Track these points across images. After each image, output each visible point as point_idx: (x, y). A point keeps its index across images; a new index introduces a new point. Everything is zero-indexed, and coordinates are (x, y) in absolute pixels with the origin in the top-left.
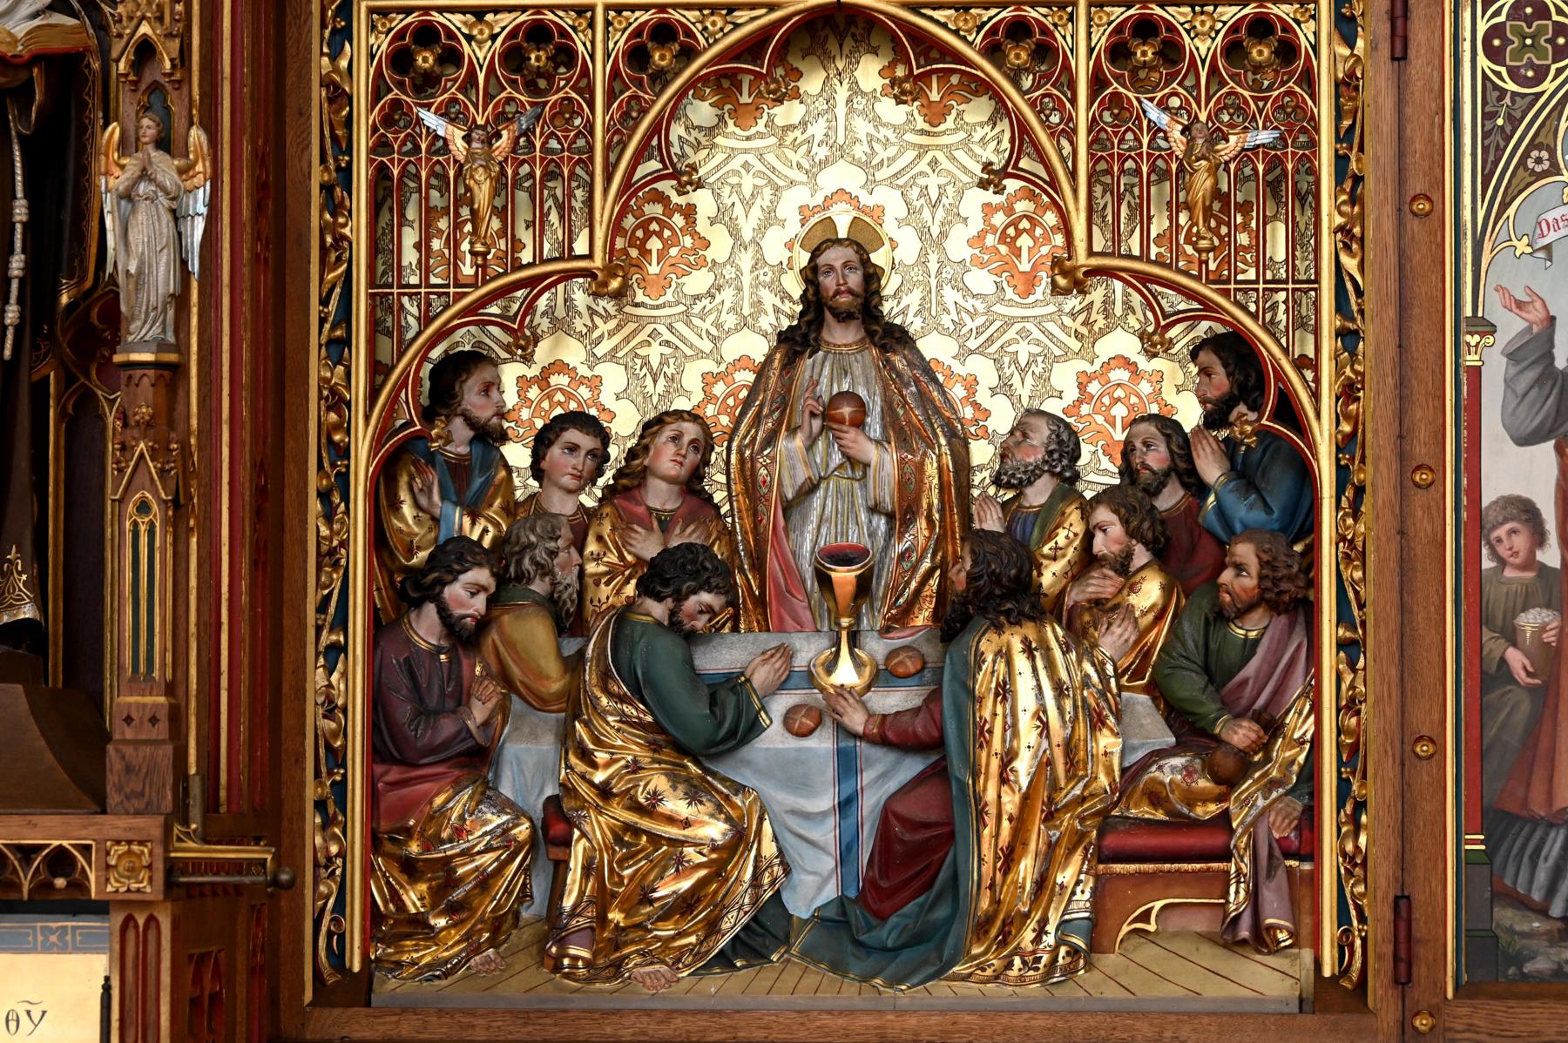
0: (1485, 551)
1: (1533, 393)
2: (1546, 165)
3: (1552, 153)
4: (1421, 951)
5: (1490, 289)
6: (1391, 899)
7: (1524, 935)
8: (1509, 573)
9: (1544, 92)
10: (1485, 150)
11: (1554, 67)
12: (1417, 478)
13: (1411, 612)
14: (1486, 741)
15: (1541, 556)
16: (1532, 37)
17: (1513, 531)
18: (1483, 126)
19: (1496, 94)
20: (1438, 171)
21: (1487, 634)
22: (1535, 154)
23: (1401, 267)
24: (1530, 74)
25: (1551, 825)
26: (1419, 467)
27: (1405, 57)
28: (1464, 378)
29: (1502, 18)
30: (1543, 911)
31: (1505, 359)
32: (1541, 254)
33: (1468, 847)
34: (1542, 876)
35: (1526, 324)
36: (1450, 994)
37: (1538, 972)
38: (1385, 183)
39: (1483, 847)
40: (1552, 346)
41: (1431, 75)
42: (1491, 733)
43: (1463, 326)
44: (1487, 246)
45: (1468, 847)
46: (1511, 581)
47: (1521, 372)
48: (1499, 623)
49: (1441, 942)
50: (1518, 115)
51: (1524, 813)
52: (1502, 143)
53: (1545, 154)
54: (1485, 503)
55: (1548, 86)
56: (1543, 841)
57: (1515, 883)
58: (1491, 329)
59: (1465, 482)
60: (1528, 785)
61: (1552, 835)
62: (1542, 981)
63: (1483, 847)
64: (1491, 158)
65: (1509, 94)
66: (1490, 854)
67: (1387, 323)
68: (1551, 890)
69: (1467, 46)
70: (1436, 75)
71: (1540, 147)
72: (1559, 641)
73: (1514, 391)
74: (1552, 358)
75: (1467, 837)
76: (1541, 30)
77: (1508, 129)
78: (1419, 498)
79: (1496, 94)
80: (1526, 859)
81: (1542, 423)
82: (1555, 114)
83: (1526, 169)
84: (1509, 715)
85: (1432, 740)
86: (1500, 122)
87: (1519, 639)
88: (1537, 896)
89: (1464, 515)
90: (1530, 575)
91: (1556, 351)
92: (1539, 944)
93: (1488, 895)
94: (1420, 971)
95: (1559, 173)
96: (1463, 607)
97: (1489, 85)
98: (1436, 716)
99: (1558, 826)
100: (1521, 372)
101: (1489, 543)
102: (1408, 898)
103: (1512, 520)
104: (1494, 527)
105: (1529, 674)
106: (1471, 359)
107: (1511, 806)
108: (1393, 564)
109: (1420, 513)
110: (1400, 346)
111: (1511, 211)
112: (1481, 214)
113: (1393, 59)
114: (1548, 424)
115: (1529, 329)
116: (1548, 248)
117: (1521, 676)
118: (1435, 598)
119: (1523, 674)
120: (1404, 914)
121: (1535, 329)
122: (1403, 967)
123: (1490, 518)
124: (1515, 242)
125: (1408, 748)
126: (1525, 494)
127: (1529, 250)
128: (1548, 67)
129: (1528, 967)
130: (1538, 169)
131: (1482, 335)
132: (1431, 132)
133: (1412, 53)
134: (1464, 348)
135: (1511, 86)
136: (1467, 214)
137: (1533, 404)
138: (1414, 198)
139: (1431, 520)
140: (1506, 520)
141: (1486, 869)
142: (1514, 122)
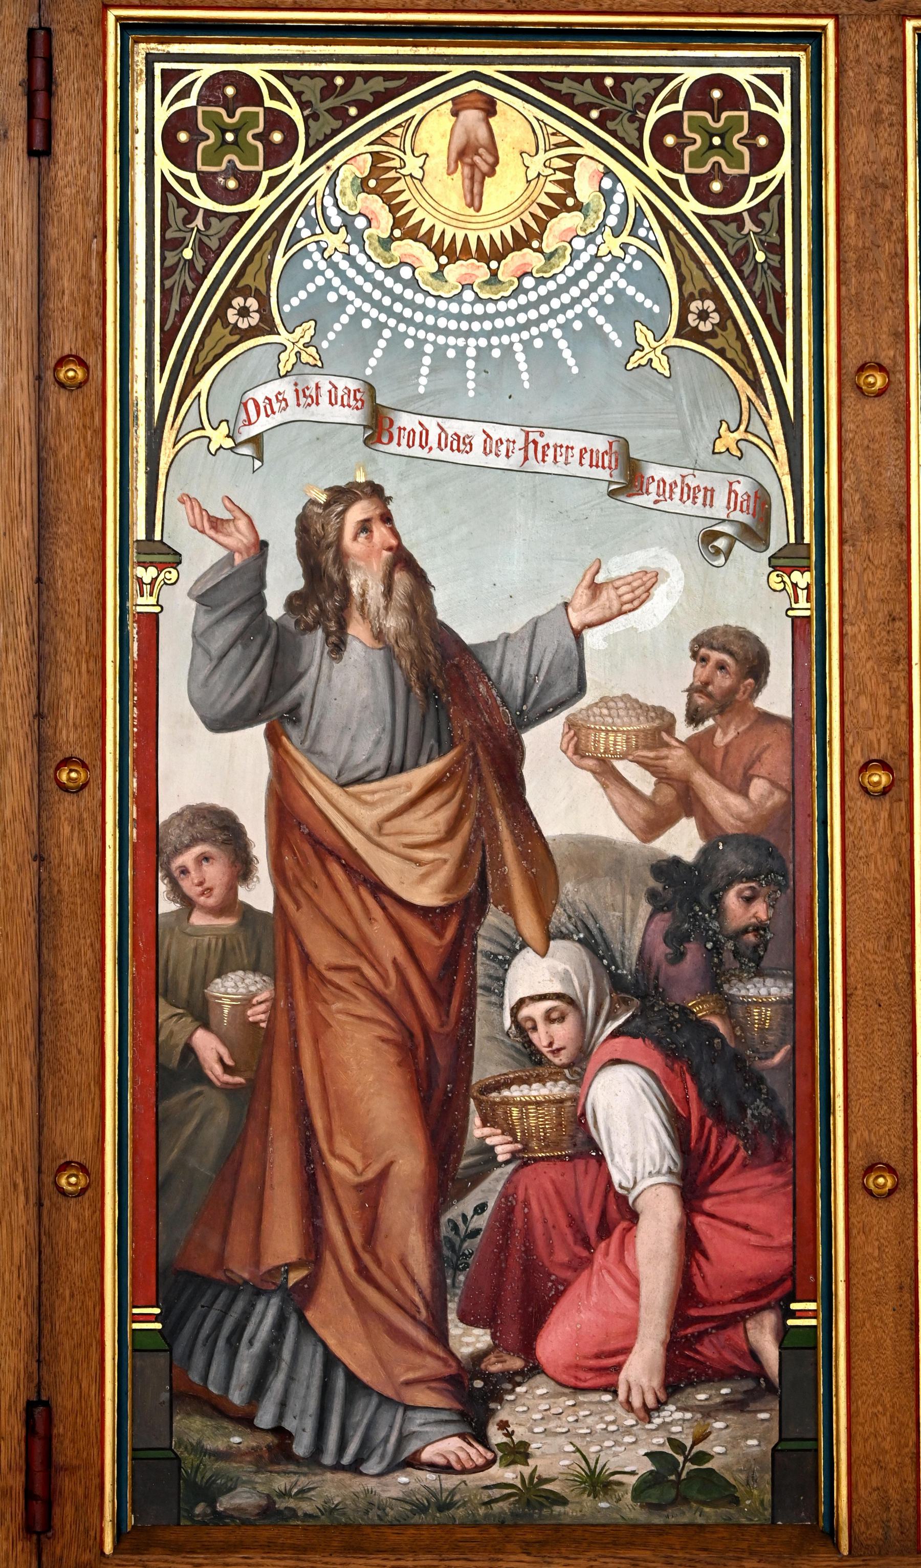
0: (163, 887)
1: (235, 654)
2: (254, 319)
3: (264, 301)
4: (66, 1483)
5: (172, 499)
6: (21, 1405)
7: (218, 1455)
8: (198, 919)
9: (251, 212)
10: (166, 294)
11: (266, 175)
12: (64, 777)
13: (54, 976)
14: (164, 1168)
15: (244, 895)
16: (236, 130)
17: (205, 858)
18: (163, 259)
19: (183, 212)
20: (96, 321)
21: (165, 1010)
22: (238, 302)
23: (41, 463)
24: (232, 184)
25: (258, 1293)
26: (66, 762)
27: (47, 151)
28: (133, 630)
29: (191, 102)
30: (246, 1420)
31: (194, 604)
32: (246, 450)
33: (136, 1326)
34: (245, 1367)
35: (224, 553)
36: (108, 1548)
37: (239, 1509)
38: (18, 337)
39: (158, 1326)
40: (263, 585)
41: (87, 180)
42: (170, 1156)
43: (133, 555)
44: (168, 436)
45: (136, 1326)
46: (200, 931)
47: (218, 622)
48: (184, 992)
49: (95, 1471)
50: (214, 244)
51: (219, 1275)
52: (190, 286)
53: (252, 303)
54: (164, 815)
55: (257, 203)
56: (246, 1316)
57: (205, 1378)
58: (173, 559)
59: (133, 784)
60: (225, 1236)
61: (260, 1307)
62: (245, 1523)
63: (158, 1326)
64: (175, 306)
65: (201, 213)
66: (169, 1335)
67: (19, 545)
68: (258, 1389)
69: (139, 140)
70: (94, 178)
71: (246, 292)
72: (269, 1020)
73: (207, 652)
74: (263, 603)
75: (135, 1311)
76: (248, 121)
77: (200, 264)
78: (67, 806)
79: (183, 212)
80: (221, 1343)
81: (248, 698)
82: (268, 244)
83: (226, 323)
84: (199, 1127)
85: (83, 1168)
86: (188, 254)
87: (213, 1021)
88: (237, 1397)
89: (133, 833)
90: (228, 922)
91: (267, 593)
92: (241, 1469)
93: (165, 1396)
94: (64, 1514)
95: (273, 331)
96: (131, 970)
97: (171, 198)
98: (90, 1133)
99: (269, 1294)
100: (218, 622)
101: (169, 875)
102: (47, 1405)
103: (203, 840)
104: (177, 852)
105: (227, 1069)
106: (144, 603)
107: (202, 1265)
108: (27, 906)
109: (67, 829)
110: (39, 580)
111: (203, 385)
112: (159, 389)
113: (31, 153)
114: (259, 696)
115: (230, 559)
116: (256, 441)
117: (215, 1071)
118: (89, 956)
119: (218, 1069)
120: (40, 1428)
121: (238, 560)
122: (38, 1508)
123: (171, 837)
124: (209, 432)
125: (47, 1180)
126: (221, 802)
127: (229, 443)
128: (259, 175)
129: (224, 1504)
130: (243, 324)
131: (160, 566)
132: (86, 264)
133: (58, 147)
134: (133, 586)
135: (204, 202)
136: (138, 389)
137: (234, 670)
138: (62, 361)
139: (84, 841)
140: (194, 842)
141: (162, 1360)
142: (208, 254)
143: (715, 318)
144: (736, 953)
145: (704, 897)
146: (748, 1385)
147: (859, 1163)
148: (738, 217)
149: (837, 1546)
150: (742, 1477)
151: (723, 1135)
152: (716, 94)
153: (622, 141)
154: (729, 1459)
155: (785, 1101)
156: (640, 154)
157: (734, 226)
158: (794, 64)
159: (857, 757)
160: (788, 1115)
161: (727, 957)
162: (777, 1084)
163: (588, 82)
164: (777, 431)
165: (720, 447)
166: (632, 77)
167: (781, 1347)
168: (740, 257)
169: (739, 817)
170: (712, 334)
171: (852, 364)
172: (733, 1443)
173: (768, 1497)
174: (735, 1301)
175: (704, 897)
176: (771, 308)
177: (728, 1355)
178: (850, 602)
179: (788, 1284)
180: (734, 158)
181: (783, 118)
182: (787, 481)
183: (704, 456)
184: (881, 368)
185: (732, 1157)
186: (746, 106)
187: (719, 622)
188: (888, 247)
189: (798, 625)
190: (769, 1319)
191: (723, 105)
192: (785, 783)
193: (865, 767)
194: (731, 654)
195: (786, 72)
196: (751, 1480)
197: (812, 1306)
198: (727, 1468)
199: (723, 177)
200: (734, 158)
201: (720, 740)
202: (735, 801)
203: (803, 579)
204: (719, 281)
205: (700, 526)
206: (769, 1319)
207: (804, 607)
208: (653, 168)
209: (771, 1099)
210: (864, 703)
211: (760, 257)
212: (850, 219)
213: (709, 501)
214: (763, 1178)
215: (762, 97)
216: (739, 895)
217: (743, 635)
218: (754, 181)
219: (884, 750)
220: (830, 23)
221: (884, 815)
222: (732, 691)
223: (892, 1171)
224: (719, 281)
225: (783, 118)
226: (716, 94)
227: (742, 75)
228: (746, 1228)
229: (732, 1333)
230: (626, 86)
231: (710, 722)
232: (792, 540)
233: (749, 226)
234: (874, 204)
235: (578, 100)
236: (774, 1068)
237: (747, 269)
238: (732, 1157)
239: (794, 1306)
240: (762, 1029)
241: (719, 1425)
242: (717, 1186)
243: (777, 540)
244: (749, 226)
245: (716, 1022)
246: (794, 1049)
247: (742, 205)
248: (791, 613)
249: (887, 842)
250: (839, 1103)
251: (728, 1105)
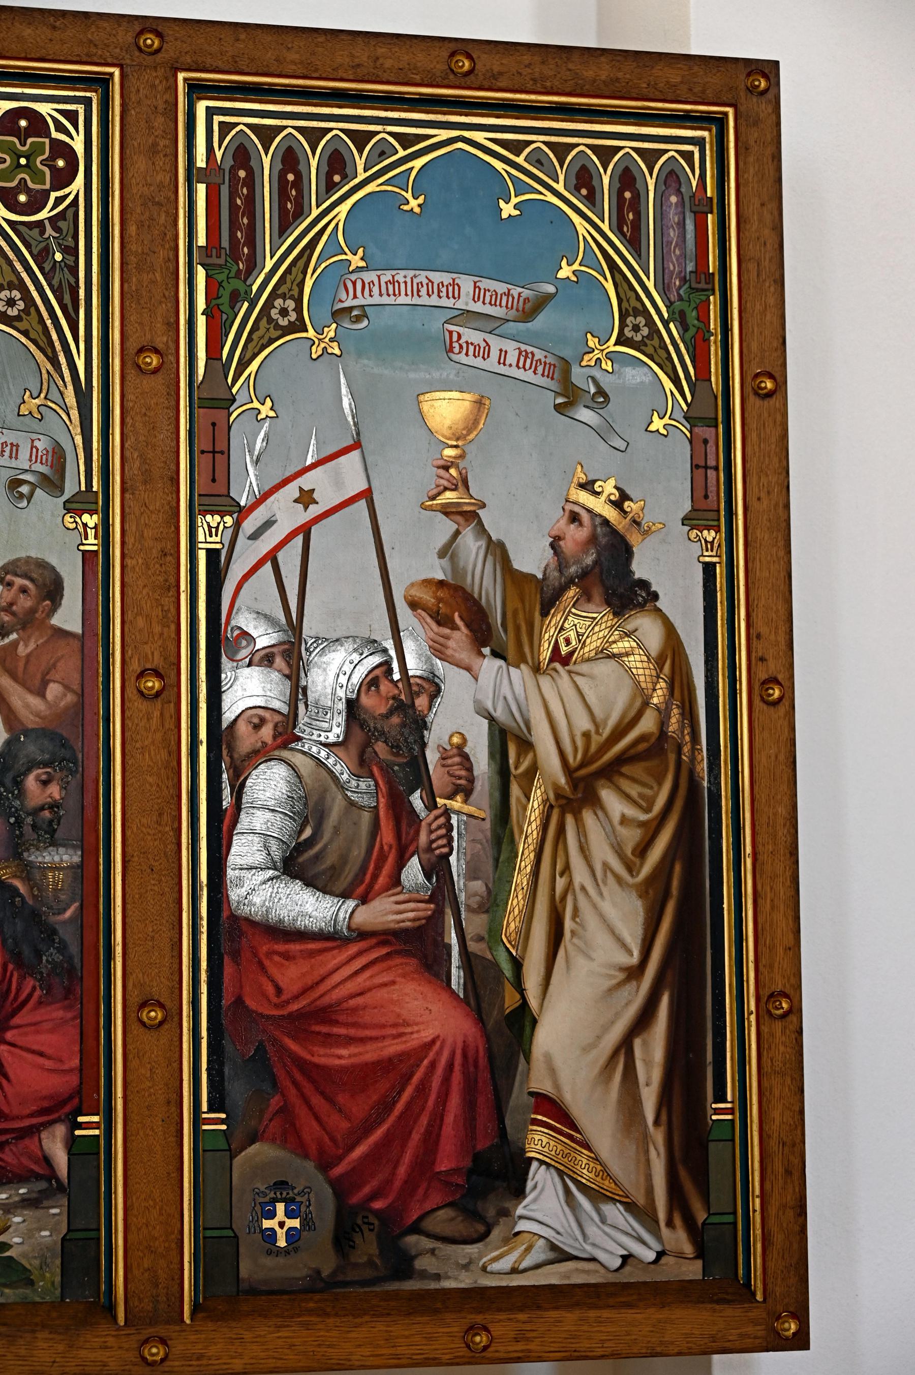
143: (21, 305)
144: (34, 827)
145: (8, 781)
146: (43, 1185)
147: (135, 1000)
148: (40, 224)
149: (115, 1318)
150: (36, 1262)
151: (22, 978)
152: (23, 123)
154: (26, 1248)
155: (74, 949)
157: (36, 231)
158: (87, 102)
159: (135, 666)
160: (77, 960)
161: (27, 830)
162: (68, 935)
164: (71, 399)
165: (24, 410)
167: (70, 1153)
168: (42, 256)
169: (37, 715)
170: (18, 318)
171: (133, 346)
172: (29, 1235)
173: (58, 1279)
174: (31, 1115)
175: (8, 781)
176: (67, 299)
177: (25, 1161)
178: (130, 540)
179: (76, 1100)
180: (37, 176)
181: (78, 145)
182: (79, 440)
183: (11, 418)
184: (157, 351)
185: (30, 996)
186: (48, 134)
187: (23, 554)
188: (162, 254)
189: (88, 557)
190: (60, 1130)
192: (76, 687)
193: (141, 675)
194: (32, 580)
195: (81, 109)
196: (44, 1265)
197: (96, 1119)
198: (24, 1255)
199: (28, 191)
200: (37, 176)
201: (22, 651)
202: (34, 701)
203: (91, 520)
204: (24, 275)
205: (7, 475)
206: (60, 1130)
207: (92, 543)
209: (63, 948)
210: (141, 622)
211: (58, 257)
212: (132, 229)
213: (14, 455)
214: (57, 1013)
215: (60, 128)
216: (37, 779)
217: (43, 565)
218: (54, 195)
219: (157, 661)
221: (157, 714)
222: (33, 611)
223: (162, 1006)
224: (24, 275)
225: (78, 145)
226: (23, 123)
227: (44, 109)
228: (41, 1054)
229: (30, 1144)
231: (14, 636)
232: (83, 488)
233: (49, 231)
234: (152, 219)
236: (64, 922)
237: (47, 267)
238: (30, 996)
239: (81, 1119)
240: (55, 890)
241: (17, 1219)
242: (16, 1021)
243: (70, 489)
244: (49, 231)
245: (18, 883)
246: (82, 905)
248: (81, 548)
249: (159, 736)
250: (119, 950)
251: (27, 951)
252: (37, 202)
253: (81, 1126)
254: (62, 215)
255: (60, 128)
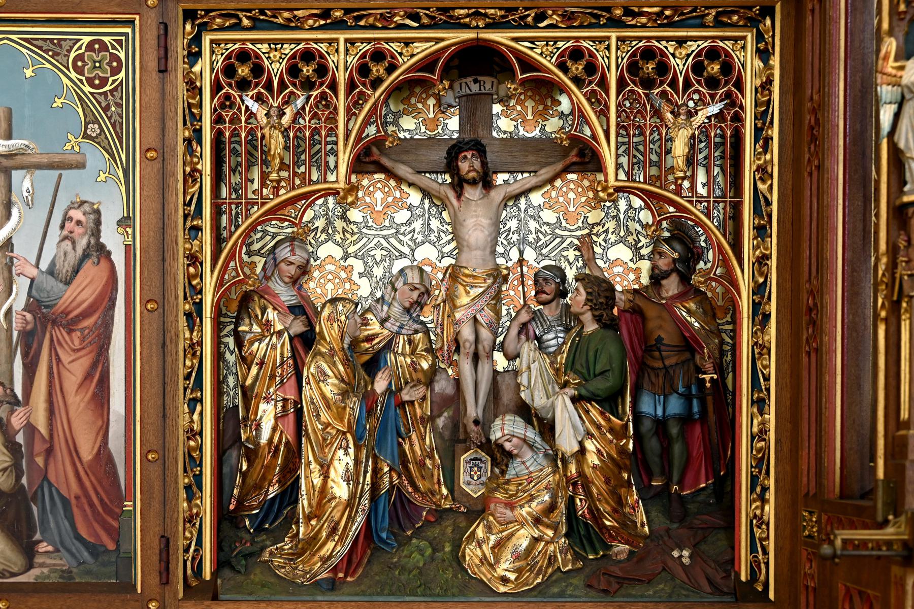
148: (105, 93)
153: (61, 64)
156: (68, 69)
163: (48, 41)
164: (121, 174)
166: (65, 40)
168: (106, 109)
176: (118, 129)
191: (100, 50)
203: (130, 230)
208: (73, 75)
211: (113, 109)
215: (114, 48)
220: (137, 17)
225: (122, 55)
227: (106, 39)
230: (62, 43)
232: (126, 215)
233: (110, 97)
235: (44, 49)
244: (110, 97)
247: (107, 88)
248: (125, 243)
252: (104, 82)
253: (125, 506)
254: (115, 89)
255: (114, 48)
